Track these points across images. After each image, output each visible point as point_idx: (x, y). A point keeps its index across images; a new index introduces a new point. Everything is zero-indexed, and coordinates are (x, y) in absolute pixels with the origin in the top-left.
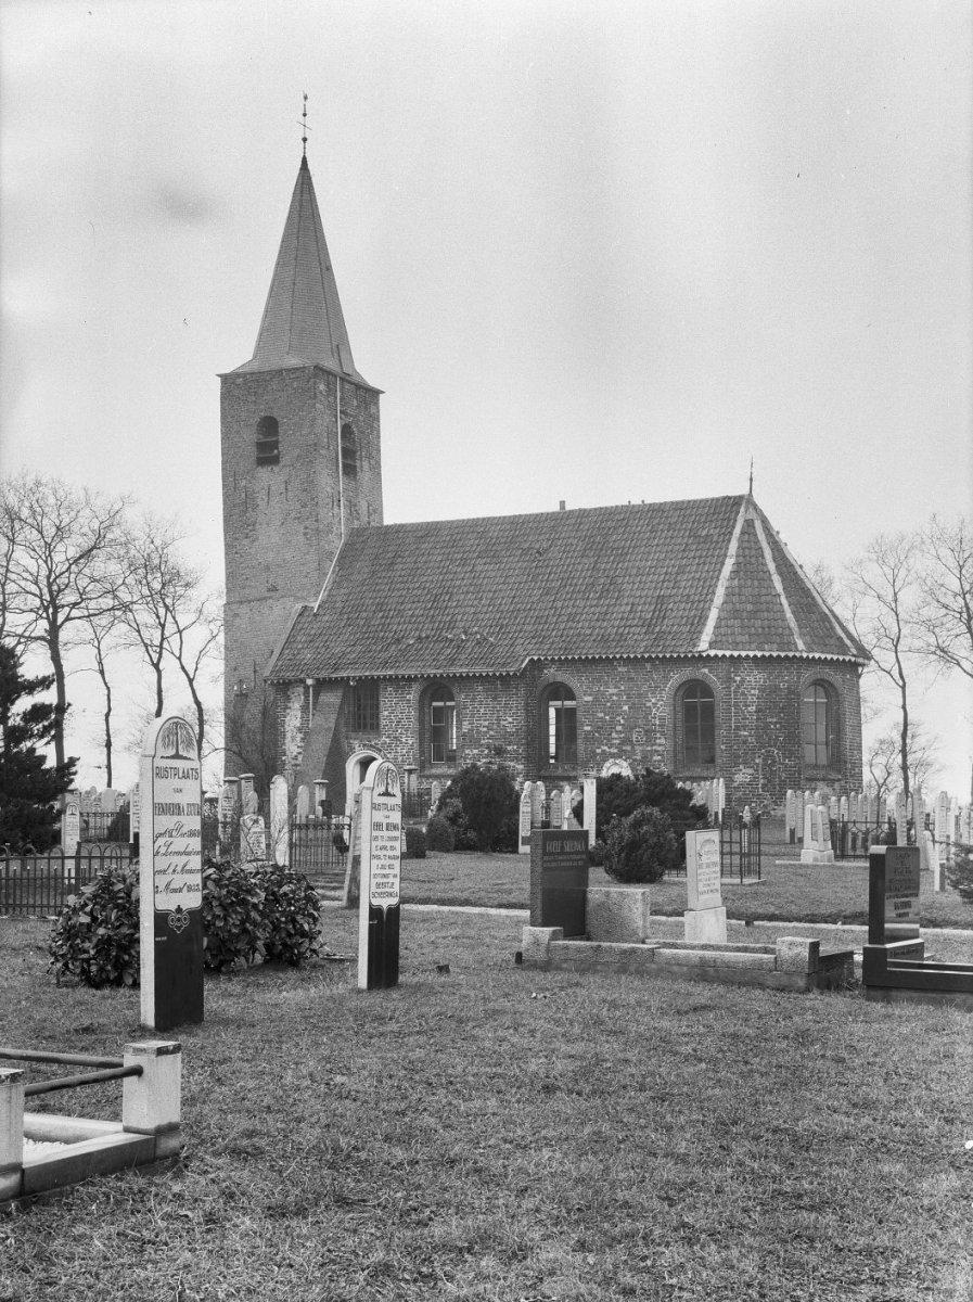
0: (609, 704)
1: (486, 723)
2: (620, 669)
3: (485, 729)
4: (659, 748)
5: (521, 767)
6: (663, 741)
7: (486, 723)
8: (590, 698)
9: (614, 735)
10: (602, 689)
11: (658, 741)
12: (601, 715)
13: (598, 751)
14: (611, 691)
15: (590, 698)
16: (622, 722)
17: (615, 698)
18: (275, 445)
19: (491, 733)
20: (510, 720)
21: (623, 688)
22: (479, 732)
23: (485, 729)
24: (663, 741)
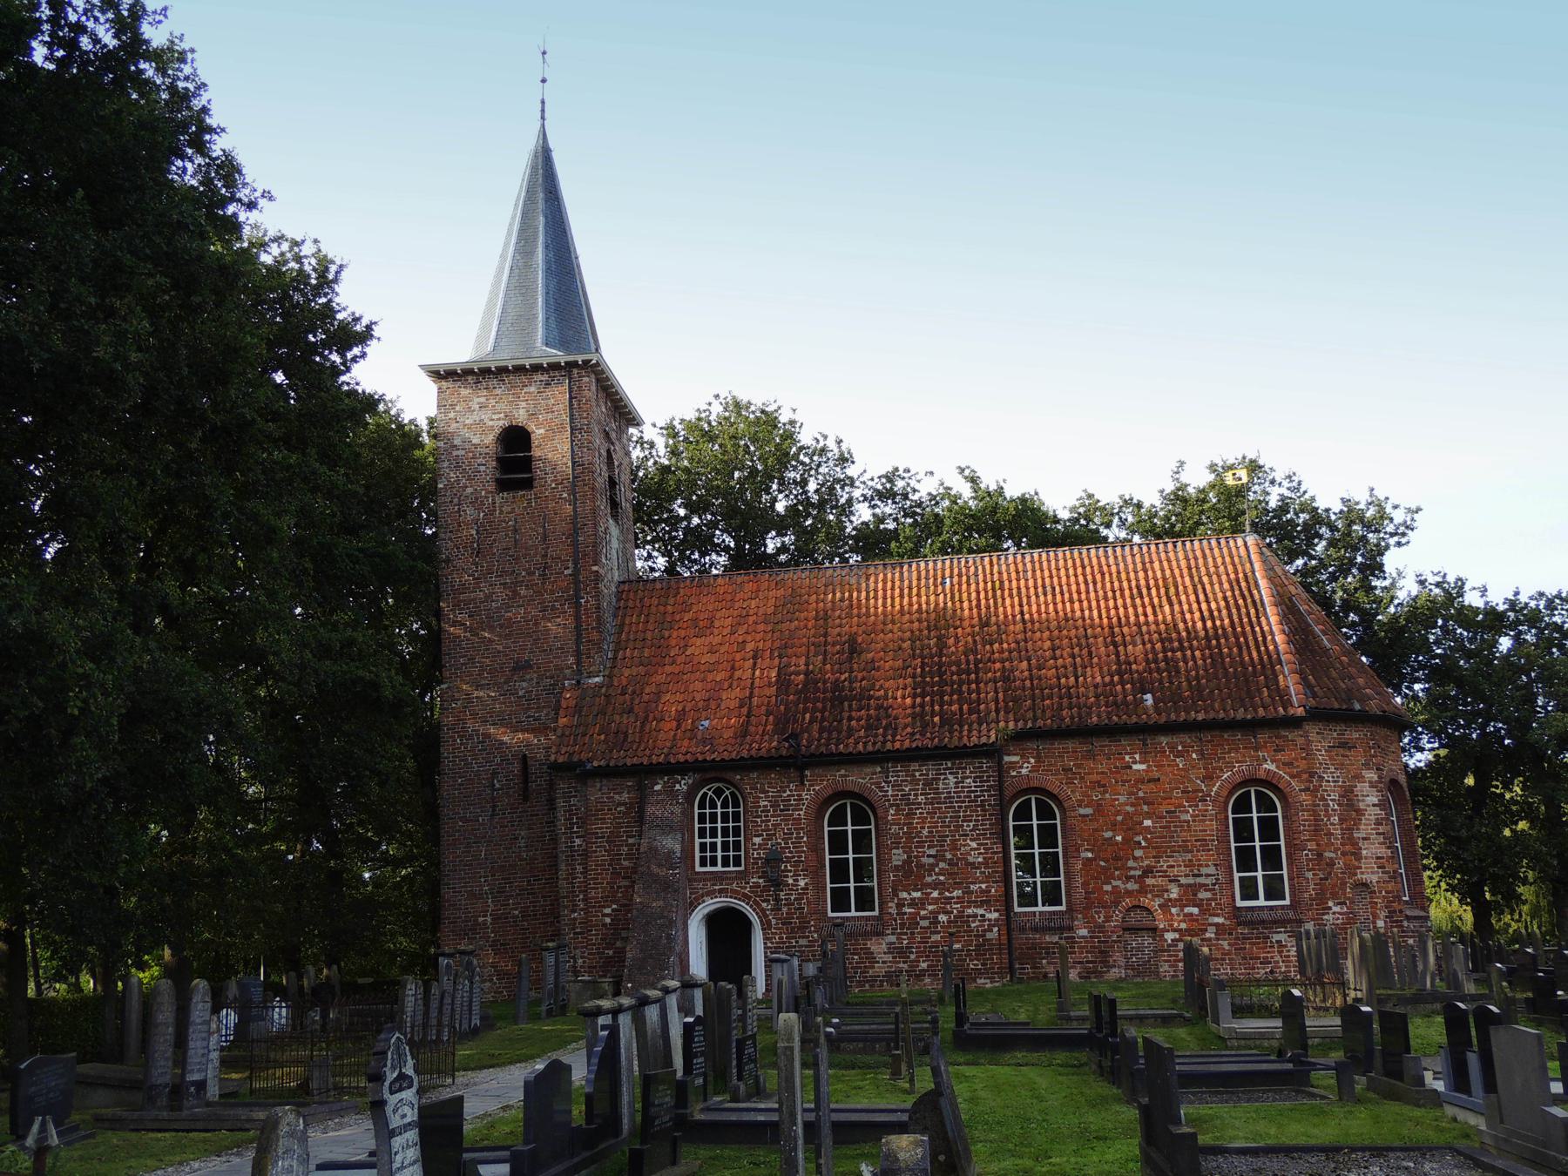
0: (1119, 818)
1: (933, 852)
2: (1135, 767)
3: (931, 860)
4: (1208, 881)
5: (995, 915)
6: (1212, 870)
7: (933, 852)
8: (1089, 811)
9: (1131, 863)
10: (1107, 796)
11: (1204, 871)
12: (1108, 834)
13: (1108, 888)
14: (1122, 799)
15: (1089, 811)
16: (1143, 844)
17: (1129, 809)
18: (526, 464)
19: (942, 865)
20: (974, 845)
21: (1141, 794)
22: (920, 866)
23: (931, 860)
24: (1212, 870)
